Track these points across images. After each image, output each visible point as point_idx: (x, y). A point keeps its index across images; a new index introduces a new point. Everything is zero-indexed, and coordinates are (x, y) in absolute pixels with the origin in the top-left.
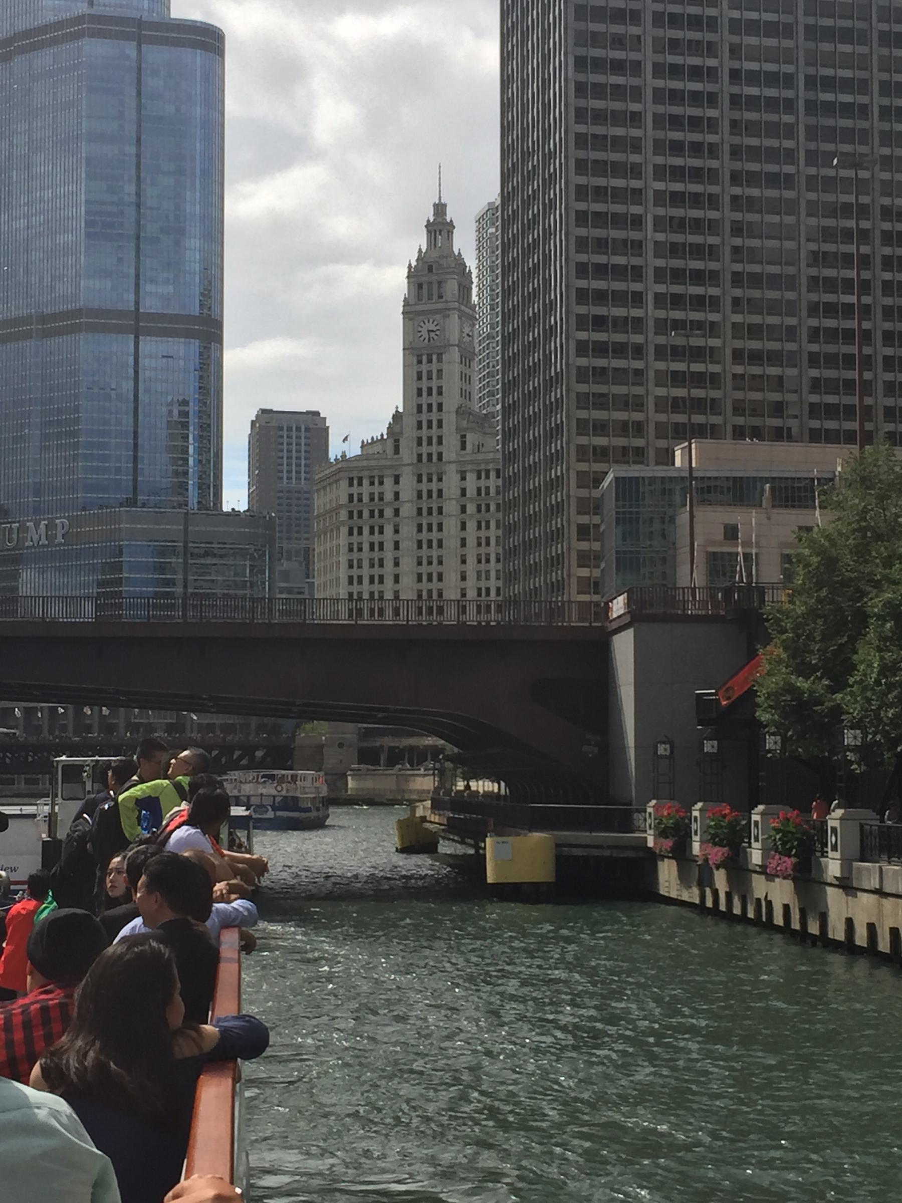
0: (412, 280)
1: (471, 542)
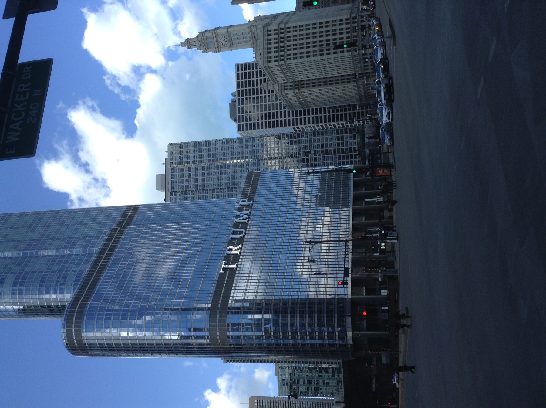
0: (207, 50)
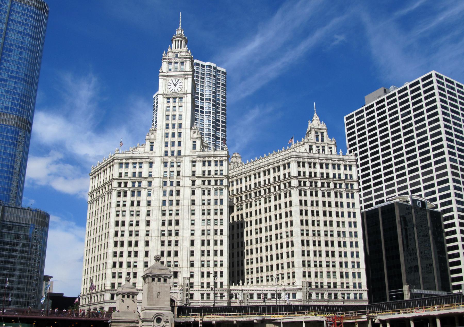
1: (198, 202)
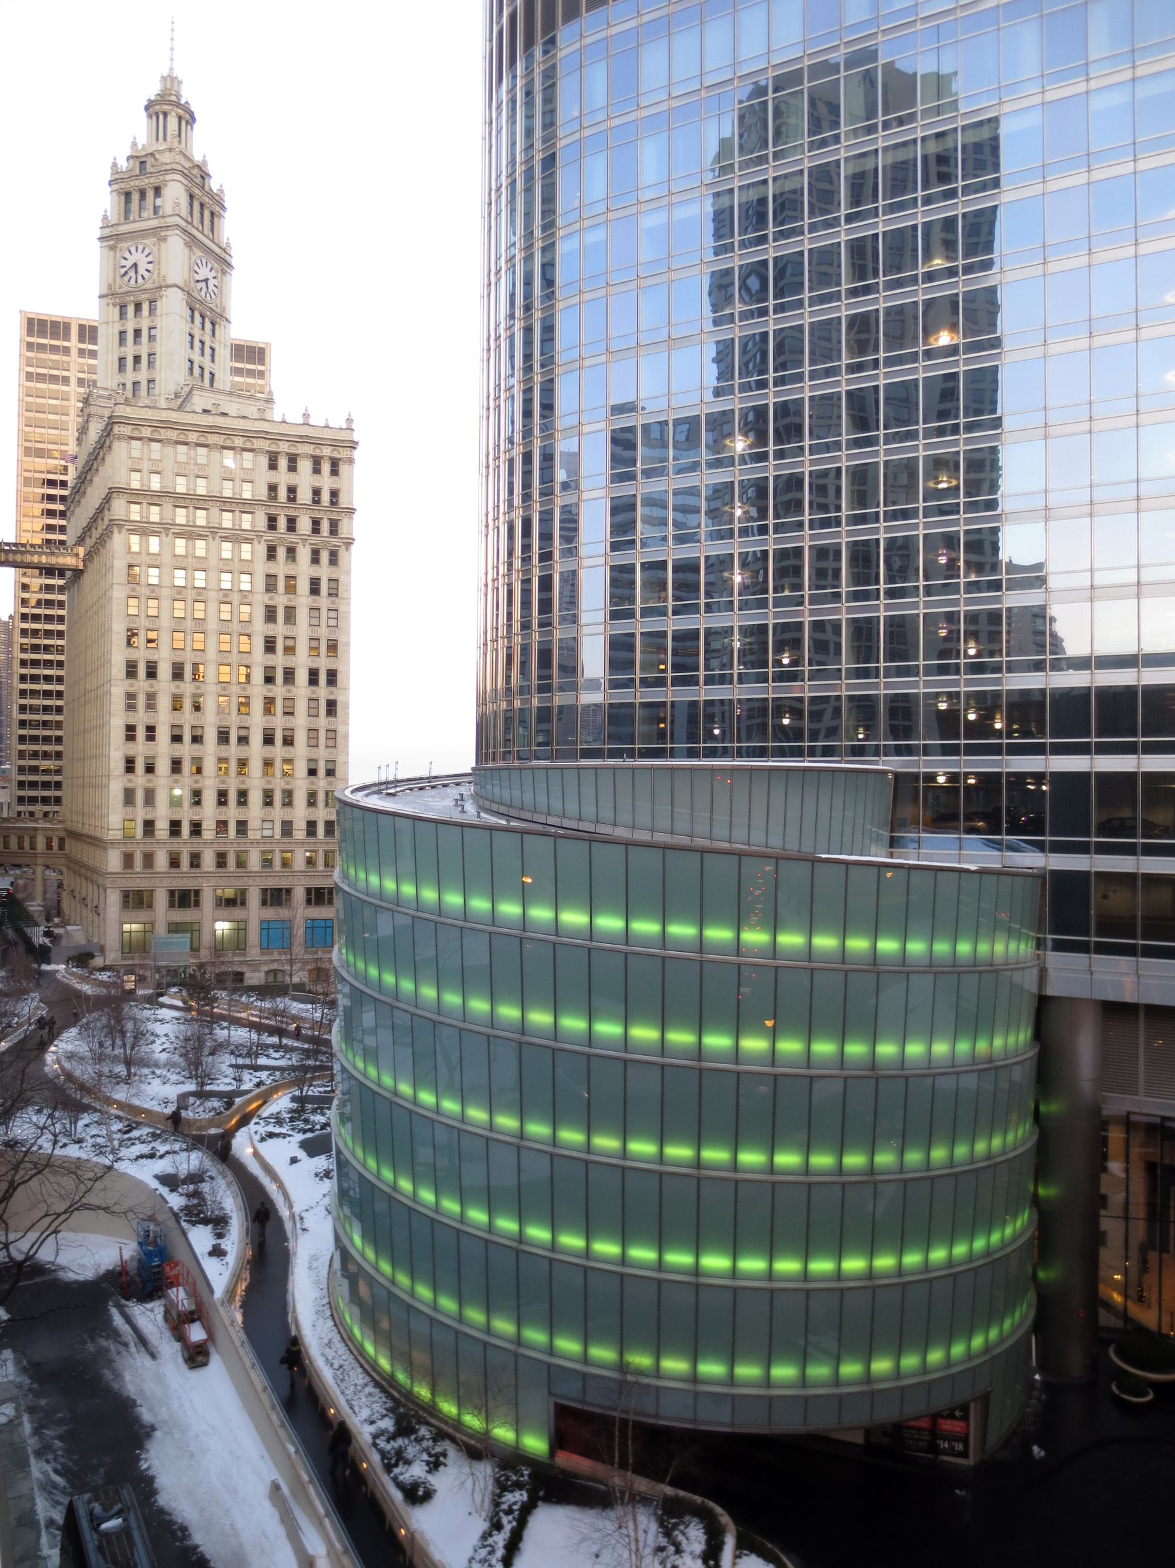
0: (116, 187)
